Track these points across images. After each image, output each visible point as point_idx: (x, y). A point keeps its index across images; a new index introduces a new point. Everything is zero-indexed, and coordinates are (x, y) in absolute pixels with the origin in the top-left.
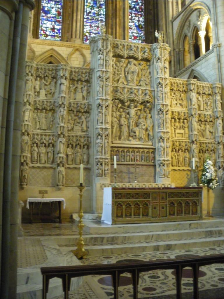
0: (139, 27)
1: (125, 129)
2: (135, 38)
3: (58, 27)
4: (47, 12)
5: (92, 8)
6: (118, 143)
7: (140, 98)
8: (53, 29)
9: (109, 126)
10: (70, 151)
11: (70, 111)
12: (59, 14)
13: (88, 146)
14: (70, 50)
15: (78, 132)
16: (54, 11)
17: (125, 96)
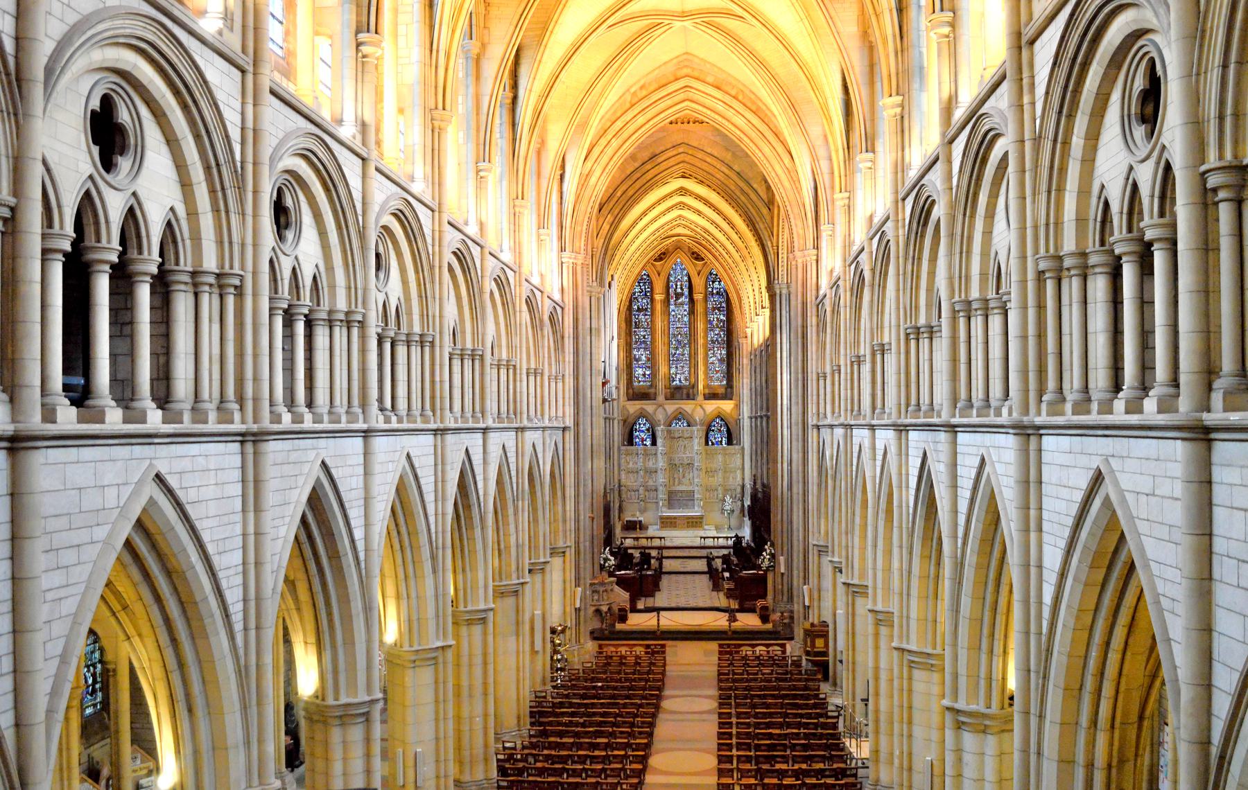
0: (721, 361)
1: (677, 480)
2: (717, 372)
3: (648, 373)
4: (638, 360)
5: (677, 349)
6: (674, 488)
7: (686, 462)
8: (644, 375)
9: (667, 480)
10: (647, 493)
11: (646, 471)
12: (648, 359)
13: (656, 490)
14: (655, 406)
15: (651, 483)
16: (643, 358)
17: (676, 462)
